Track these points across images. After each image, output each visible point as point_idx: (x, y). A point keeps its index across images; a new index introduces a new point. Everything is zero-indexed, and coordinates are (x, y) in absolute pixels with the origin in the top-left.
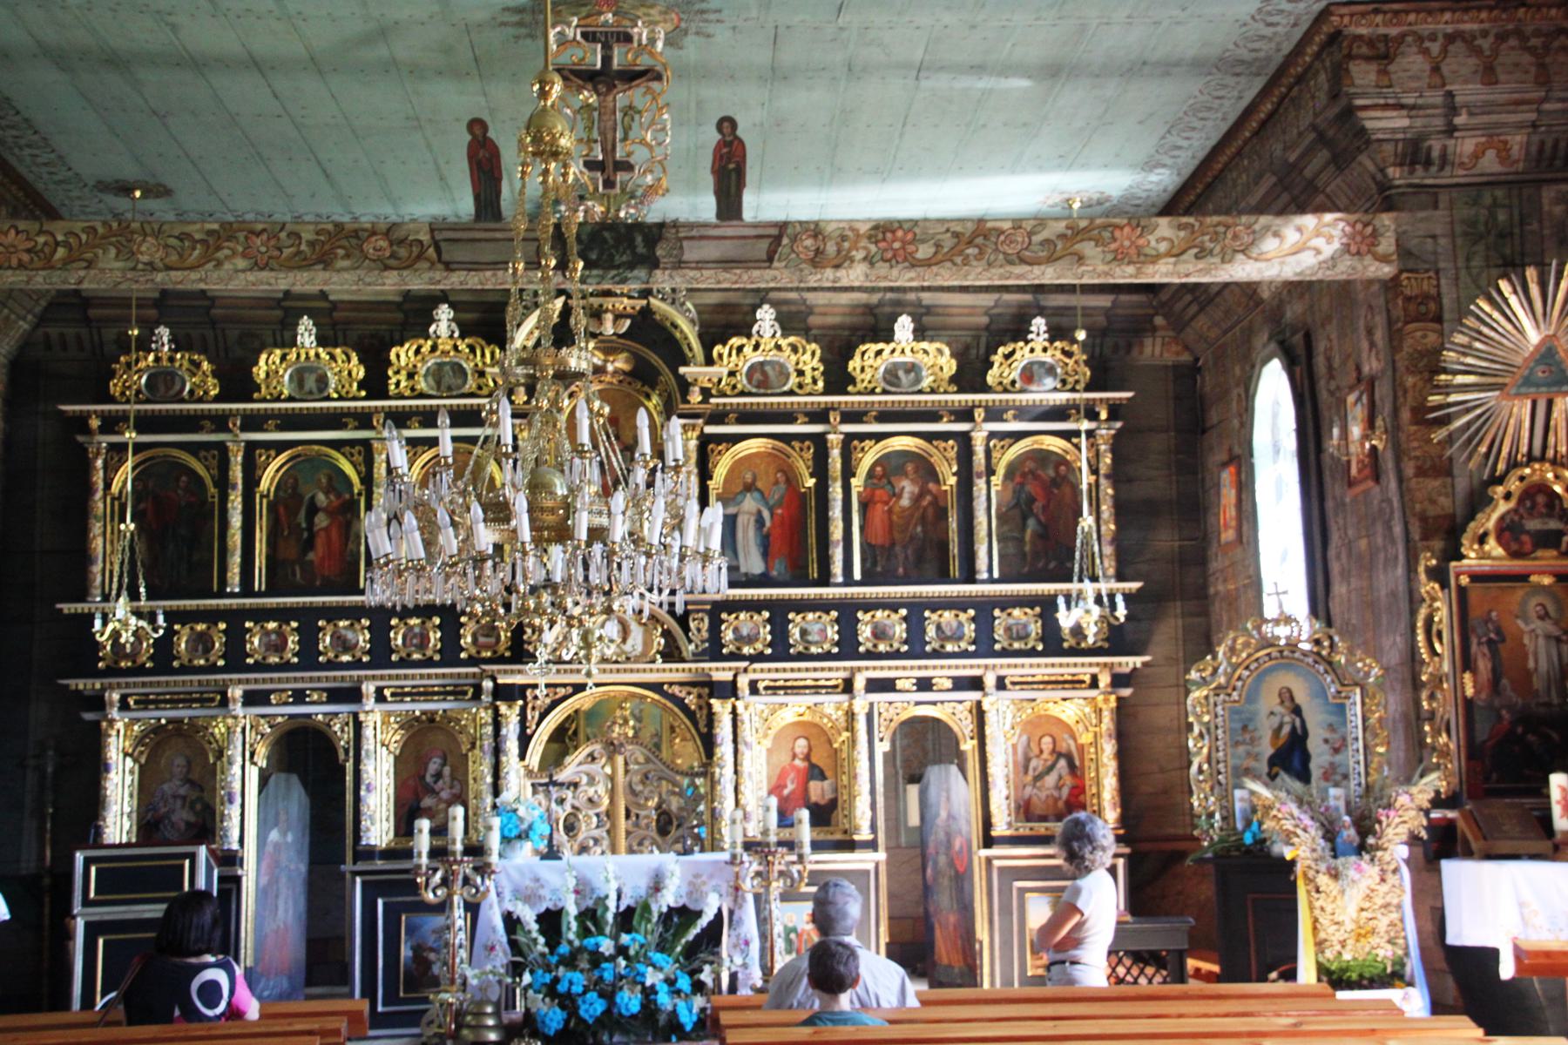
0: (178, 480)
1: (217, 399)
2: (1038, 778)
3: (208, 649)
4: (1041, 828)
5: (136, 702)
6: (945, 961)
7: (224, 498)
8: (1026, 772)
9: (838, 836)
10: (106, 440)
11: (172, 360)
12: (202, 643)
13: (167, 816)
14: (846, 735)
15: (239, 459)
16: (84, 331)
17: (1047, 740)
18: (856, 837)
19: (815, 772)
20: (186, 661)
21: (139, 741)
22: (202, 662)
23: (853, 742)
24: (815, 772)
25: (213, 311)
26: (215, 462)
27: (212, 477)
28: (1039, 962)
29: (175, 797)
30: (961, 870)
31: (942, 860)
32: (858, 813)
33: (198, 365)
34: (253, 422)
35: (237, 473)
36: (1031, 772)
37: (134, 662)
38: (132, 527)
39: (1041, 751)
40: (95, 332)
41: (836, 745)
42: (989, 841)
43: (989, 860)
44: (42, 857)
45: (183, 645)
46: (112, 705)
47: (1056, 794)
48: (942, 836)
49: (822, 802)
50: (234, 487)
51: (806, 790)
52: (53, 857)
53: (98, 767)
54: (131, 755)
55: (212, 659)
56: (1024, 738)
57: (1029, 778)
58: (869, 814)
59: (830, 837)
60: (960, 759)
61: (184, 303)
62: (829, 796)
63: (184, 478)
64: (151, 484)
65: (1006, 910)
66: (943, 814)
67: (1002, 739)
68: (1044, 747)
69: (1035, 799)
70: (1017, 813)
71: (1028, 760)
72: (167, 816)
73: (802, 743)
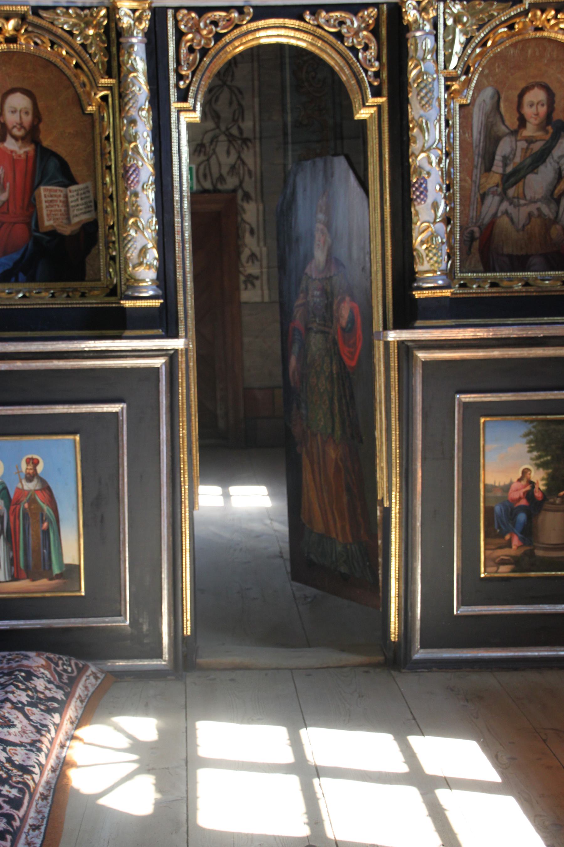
2: (514, 178)
4: (515, 282)
6: (319, 527)
8: (488, 168)
9: (94, 301)
14: (105, 81)
17: (537, 96)
18: (128, 304)
19: (50, 167)
23: (121, 94)
24: (50, 167)
28: (503, 553)
30: (351, 363)
31: (316, 342)
32: (133, 254)
36: (498, 167)
39: (523, 122)
41: (90, 109)
42: (407, 312)
43: (406, 350)
47: (545, 210)
48: (315, 296)
49: (67, 231)
51: (32, 205)
56: (488, 92)
57: (495, 179)
58: (153, 254)
59: (78, 303)
60: (349, 140)
62: (79, 217)
65: (437, 451)
66: (320, 256)
67: (443, 95)
68: (528, 111)
69: (504, 221)
70: (466, 252)
71: (492, 140)
73: (18, 101)
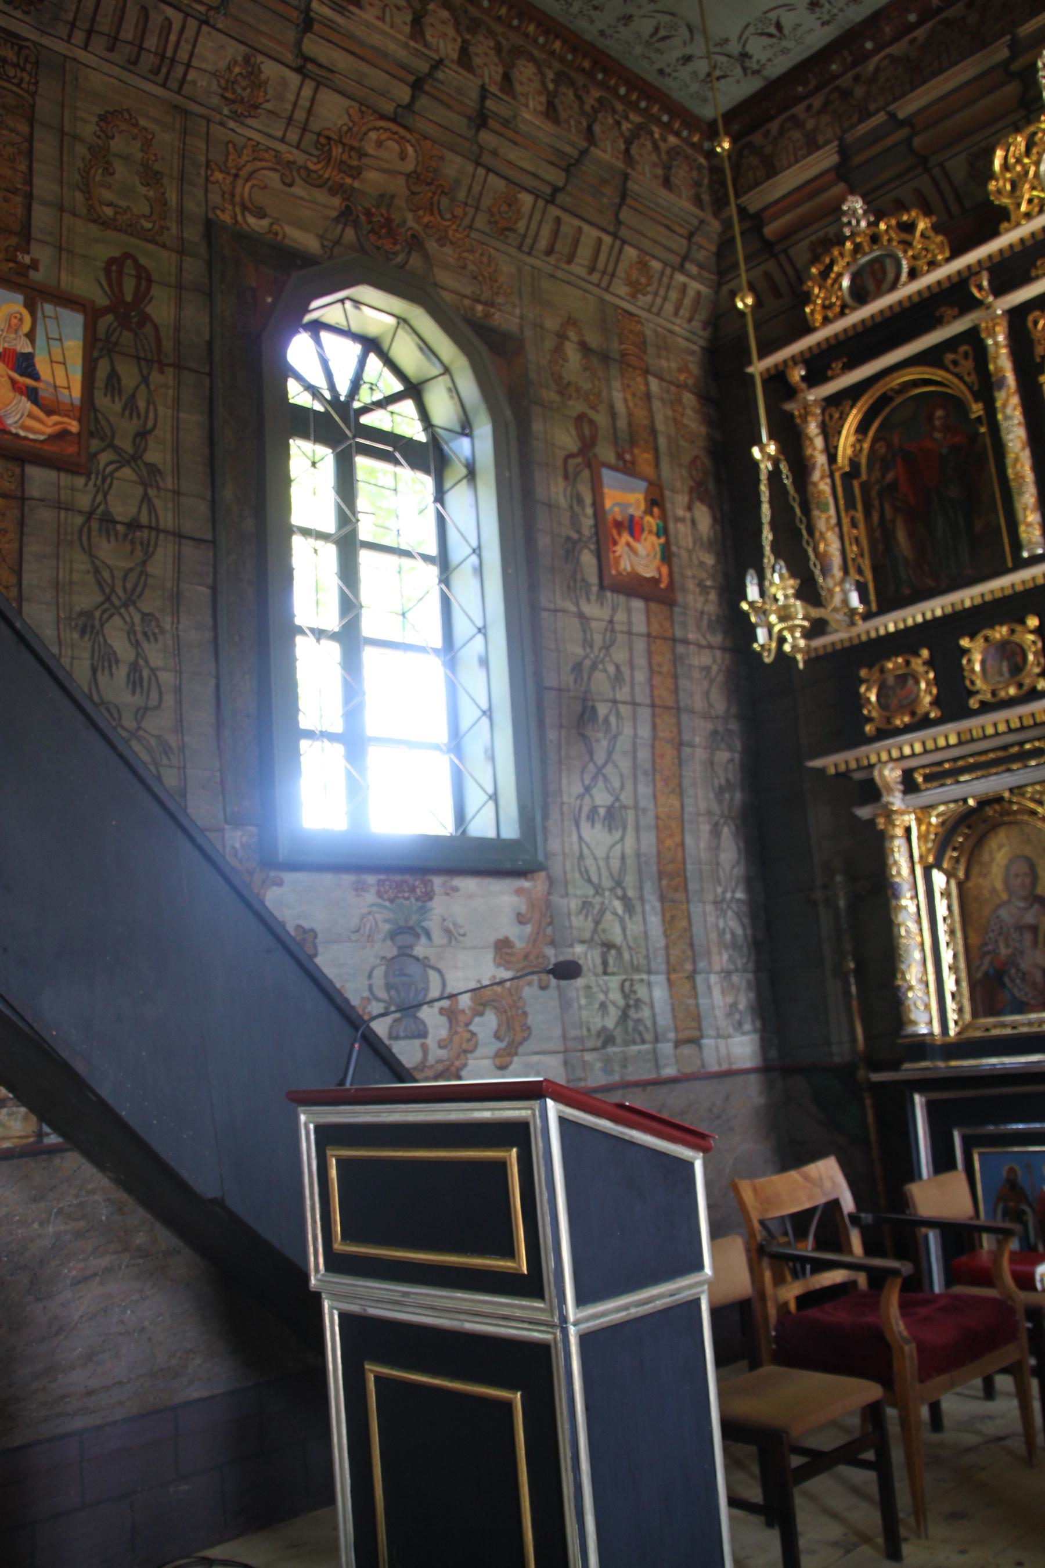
0: (930, 419)
1: (948, 260)
3: (1017, 667)
5: (927, 778)
7: (991, 410)
10: (813, 396)
11: (875, 239)
12: (1011, 656)
13: (1012, 961)
15: (1001, 338)
16: (771, 266)
20: (988, 697)
21: (944, 842)
22: (1012, 691)
25: (917, 141)
26: (968, 365)
27: (970, 388)
29: (1020, 928)
33: (909, 228)
34: (1009, 272)
35: (1003, 363)
37: (913, 714)
38: (772, 449)
40: (782, 258)
44: (854, 1040)
45: (977, 667)
46: (890, 790)
50: (1001, 383)
52: (867, 1037)
53: (877, 892)
54: (938, 865)
55: (1027, 682)
61: (878, 148)
63: (939, 413)
64: (896, 440)
72: (1012, 961)
